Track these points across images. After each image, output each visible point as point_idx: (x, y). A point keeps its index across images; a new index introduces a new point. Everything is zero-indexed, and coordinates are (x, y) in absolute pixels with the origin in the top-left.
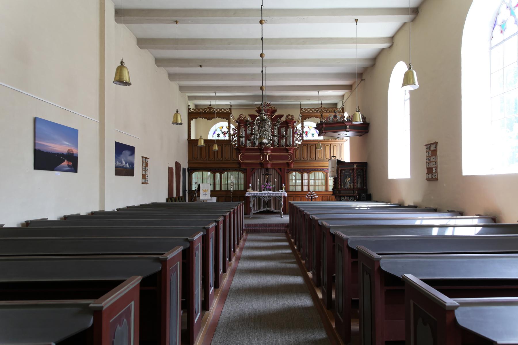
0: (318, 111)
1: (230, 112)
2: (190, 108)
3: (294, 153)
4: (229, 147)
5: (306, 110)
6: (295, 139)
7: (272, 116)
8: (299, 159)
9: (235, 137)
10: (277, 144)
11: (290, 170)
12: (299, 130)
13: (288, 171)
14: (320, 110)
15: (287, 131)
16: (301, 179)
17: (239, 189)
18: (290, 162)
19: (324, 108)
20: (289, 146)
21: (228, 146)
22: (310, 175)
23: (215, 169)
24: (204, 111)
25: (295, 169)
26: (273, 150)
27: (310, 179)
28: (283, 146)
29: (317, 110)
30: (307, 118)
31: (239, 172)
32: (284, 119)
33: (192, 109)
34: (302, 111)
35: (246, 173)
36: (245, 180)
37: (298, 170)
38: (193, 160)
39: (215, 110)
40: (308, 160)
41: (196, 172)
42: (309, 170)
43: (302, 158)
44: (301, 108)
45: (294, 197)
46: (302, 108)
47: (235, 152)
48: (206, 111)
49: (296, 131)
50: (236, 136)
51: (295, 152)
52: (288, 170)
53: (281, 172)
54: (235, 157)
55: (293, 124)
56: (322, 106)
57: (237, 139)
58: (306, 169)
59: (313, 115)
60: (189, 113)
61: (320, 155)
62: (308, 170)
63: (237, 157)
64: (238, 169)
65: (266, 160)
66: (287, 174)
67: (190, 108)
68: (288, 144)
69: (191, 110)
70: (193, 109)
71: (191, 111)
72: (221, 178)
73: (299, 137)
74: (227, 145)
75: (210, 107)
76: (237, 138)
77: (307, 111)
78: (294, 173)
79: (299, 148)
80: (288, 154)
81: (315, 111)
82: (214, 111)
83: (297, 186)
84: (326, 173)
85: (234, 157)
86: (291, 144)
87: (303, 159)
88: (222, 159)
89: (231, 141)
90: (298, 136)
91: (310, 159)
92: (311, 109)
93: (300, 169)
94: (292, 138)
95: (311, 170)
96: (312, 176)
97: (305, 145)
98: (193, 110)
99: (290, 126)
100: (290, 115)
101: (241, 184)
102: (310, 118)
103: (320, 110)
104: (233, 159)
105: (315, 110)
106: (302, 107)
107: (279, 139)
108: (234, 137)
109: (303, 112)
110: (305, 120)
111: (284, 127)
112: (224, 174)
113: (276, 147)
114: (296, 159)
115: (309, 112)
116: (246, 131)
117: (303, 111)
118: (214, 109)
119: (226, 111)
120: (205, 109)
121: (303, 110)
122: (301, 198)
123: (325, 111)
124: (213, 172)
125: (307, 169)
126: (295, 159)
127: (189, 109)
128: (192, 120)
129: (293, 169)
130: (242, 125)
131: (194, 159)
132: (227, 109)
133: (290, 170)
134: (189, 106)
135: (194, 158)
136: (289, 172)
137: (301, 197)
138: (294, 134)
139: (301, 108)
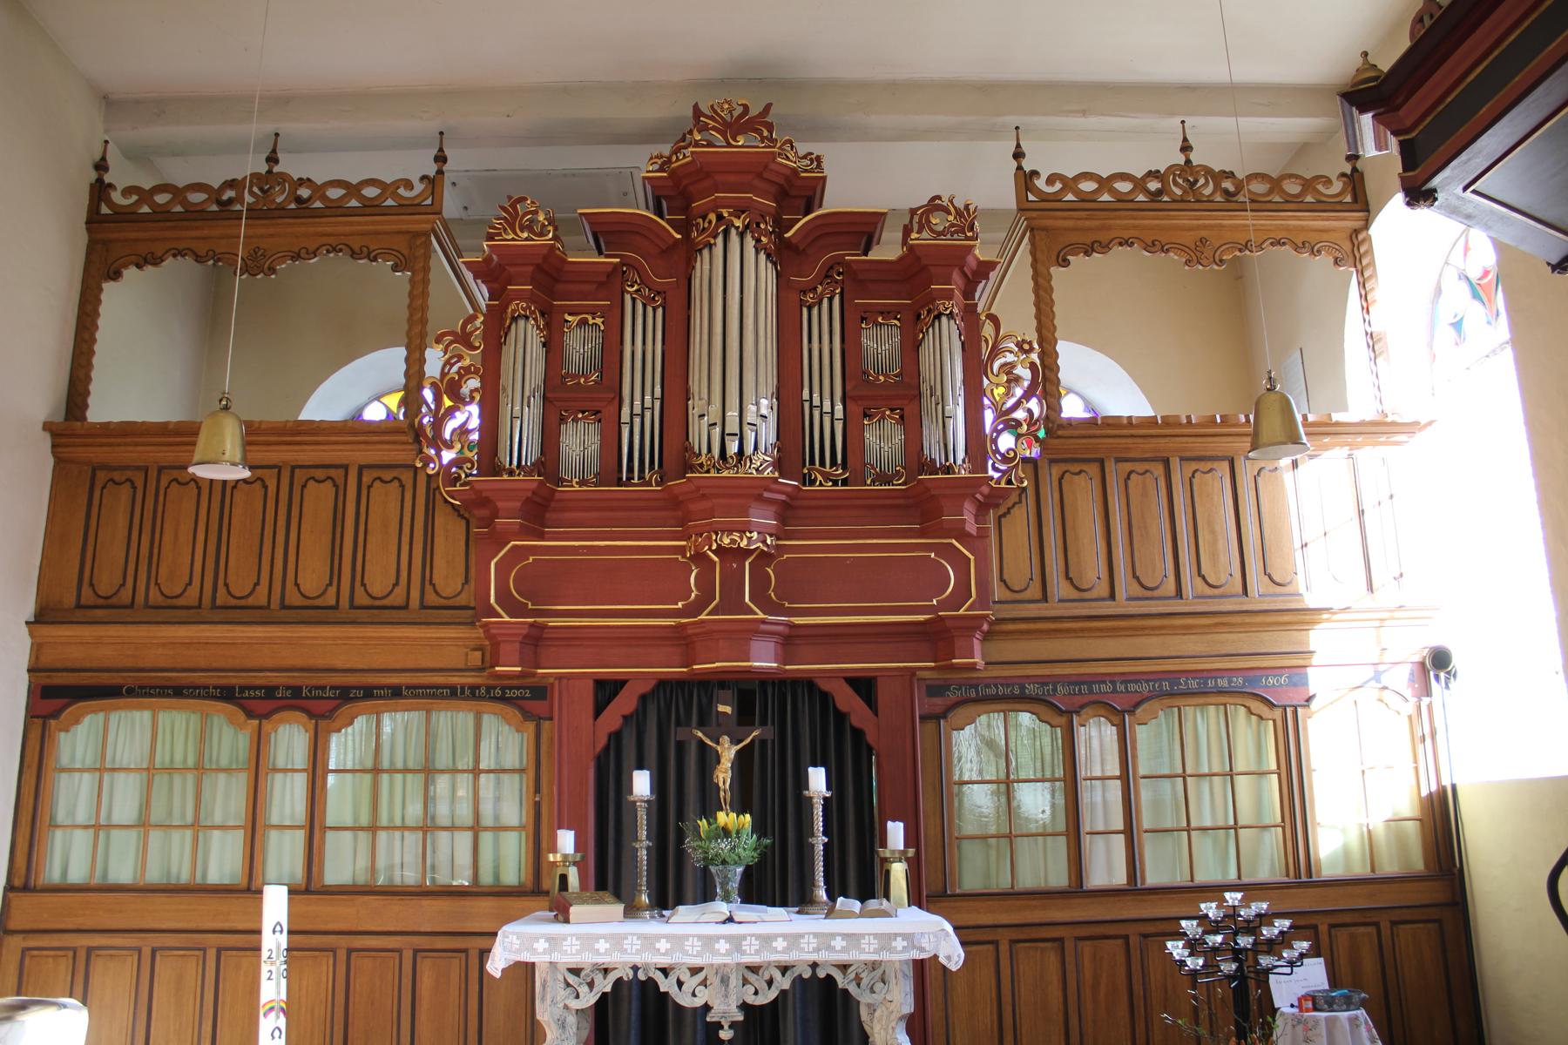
0: (1159, 192)
1: (429, 201)
2: (111, 186)
3: (983, 534)
4: (402, 486)
5: (1069, 184)
6: (989, 416)
7: (781, 226)
8: (1034, 591)
9: (460, 401)
10: (834, 463)
11: (952, 696)
12: (1019, 345)
13: (939, 703)
14: (1178, 192)
15: (917, 345)
16: (1059, 773)
17: (486, 878)
18: (961, 612)
19: (1208, 171)
20: (948, 470)
21: (396, 483)
22: (1143, 735)
23: (270, 691)
24: (219, 203)
25: (1007, 682)
26: (789, 512)
27: (1142, 771)
28: (884, 478)
29: (1154, 185)
30: (1077, 255)
31: (486, 718)
32: (888, 249)
33: (120, 188)
34: (1031, 197)
35: (546, 725)
36: (537, 790)
37: (1031, 689)
38: (79, 606)
39: (304, 192)
40: (1112, 596)
41: (101, 716)
42: (1132, 687)
43: (1064, 585)
44: (1020, 168)
45: (1004, 948)
46: (1035, 173)
47: (449, 535)
48: (231, 201)
49: (995, 352)
50: (465, 390)
51: (992, 526)
52: (935, 690)
53: (876, 715)
54: (448, 578)
55: (969, 293)
56: (1188, 162)
57: (474, 423)
58: (1101, 678)
59: (1126, 228)
60: (94, 220)
61: (1214, 556)
62: (1122, 688)
63: (467, 581)
64: (474, 688)
65: (732, 602)
66: (930, 726)
67: (107, 179)
68: (933, 451)
69: (116, 197)
70: (128, 191)
71: (110, 204)
72: (316, 770)
73: (1027, 395)
74: (388, 475)
75: (270, 172)
76: (474, 409)
77: (1070, 197)
78: (991, 723)
79: (1031, 493)
80: (929, 547)
81: (1141, 198)
82: (299, 200)
83: (1023, 845)
84: (1278, 713)
85: (436, 580)
86: (961, 454)
87: (1074, 594)
88: (332, 590)
89: (418, 433)
90: (1019, 392)
91: (1137, 590)
92: (1105, 183)
93: (1043, 681)
94: (961, 401)
95: (1145, 688)
96: (1151, 737)
97: (1075, 468)
98: (135, 198)
99: (949, 295)
100: (945, 202)
101: (499, 829)
102: (1105, 247)
103: (1178, 192)
104: (431, 599)
105: (1139, 184)
106: (1028, 166)
107: (845, 420)
108: (448, 403)
109: (1044, 198)
110: (1066, 263)
111: (888, 313)
112: (350, 729)
113: (821, 485)
114: (1008, 595)
115: (1085, 198)
116: (553, 346)
117: (1038, 192)
118: (302, 182)
119: (395, 195)
120: (231, 184)
121: (1040, 183)
122: (1070, 959)
123: (1218, 198)
124: (250, 714)
125: (1111, 677)
126: (998, 592)
127: (100, 190)
128: (116, 275)
129: (996, 681)
130: (520, 296)
131: (87, 596)
132: (408, 185)
133: (952, 696)
134: (101, 166)
135: (92, 585)
136: (944, 715)
137: (1069, 945)
138: (975, 370)
139: (1020, 168)
